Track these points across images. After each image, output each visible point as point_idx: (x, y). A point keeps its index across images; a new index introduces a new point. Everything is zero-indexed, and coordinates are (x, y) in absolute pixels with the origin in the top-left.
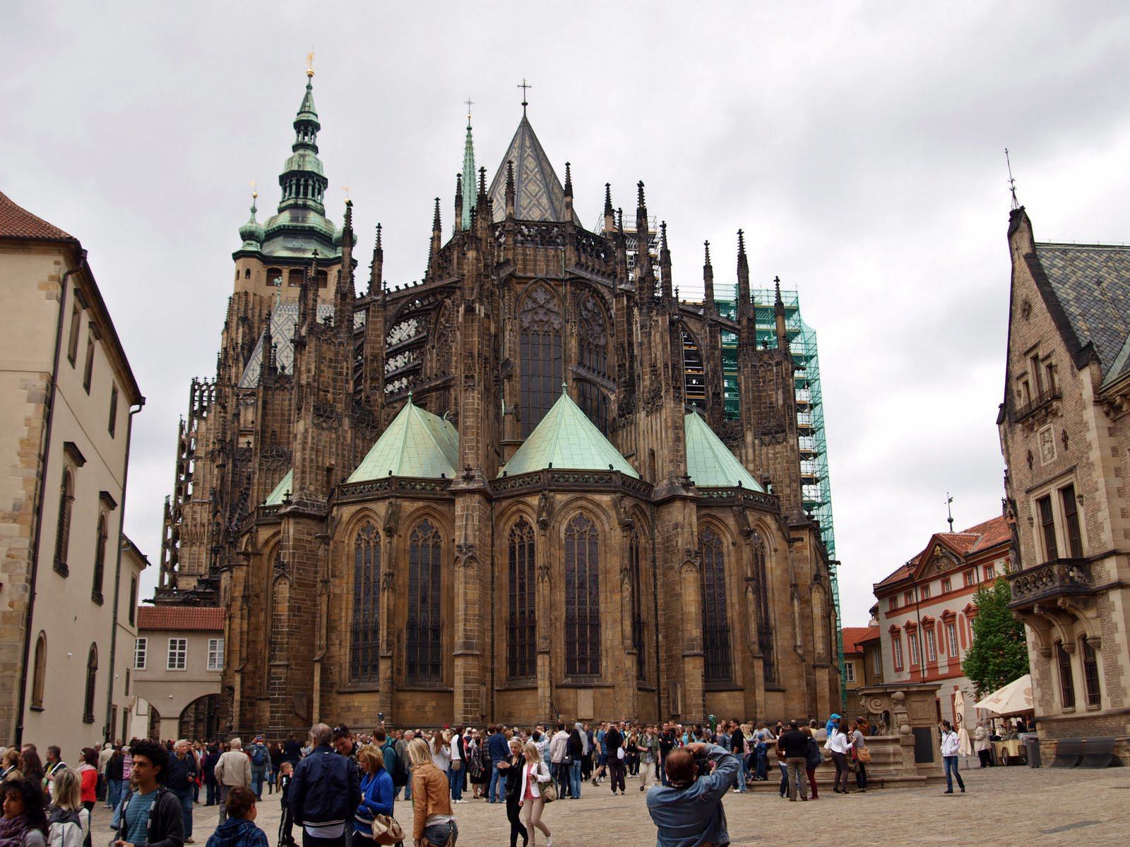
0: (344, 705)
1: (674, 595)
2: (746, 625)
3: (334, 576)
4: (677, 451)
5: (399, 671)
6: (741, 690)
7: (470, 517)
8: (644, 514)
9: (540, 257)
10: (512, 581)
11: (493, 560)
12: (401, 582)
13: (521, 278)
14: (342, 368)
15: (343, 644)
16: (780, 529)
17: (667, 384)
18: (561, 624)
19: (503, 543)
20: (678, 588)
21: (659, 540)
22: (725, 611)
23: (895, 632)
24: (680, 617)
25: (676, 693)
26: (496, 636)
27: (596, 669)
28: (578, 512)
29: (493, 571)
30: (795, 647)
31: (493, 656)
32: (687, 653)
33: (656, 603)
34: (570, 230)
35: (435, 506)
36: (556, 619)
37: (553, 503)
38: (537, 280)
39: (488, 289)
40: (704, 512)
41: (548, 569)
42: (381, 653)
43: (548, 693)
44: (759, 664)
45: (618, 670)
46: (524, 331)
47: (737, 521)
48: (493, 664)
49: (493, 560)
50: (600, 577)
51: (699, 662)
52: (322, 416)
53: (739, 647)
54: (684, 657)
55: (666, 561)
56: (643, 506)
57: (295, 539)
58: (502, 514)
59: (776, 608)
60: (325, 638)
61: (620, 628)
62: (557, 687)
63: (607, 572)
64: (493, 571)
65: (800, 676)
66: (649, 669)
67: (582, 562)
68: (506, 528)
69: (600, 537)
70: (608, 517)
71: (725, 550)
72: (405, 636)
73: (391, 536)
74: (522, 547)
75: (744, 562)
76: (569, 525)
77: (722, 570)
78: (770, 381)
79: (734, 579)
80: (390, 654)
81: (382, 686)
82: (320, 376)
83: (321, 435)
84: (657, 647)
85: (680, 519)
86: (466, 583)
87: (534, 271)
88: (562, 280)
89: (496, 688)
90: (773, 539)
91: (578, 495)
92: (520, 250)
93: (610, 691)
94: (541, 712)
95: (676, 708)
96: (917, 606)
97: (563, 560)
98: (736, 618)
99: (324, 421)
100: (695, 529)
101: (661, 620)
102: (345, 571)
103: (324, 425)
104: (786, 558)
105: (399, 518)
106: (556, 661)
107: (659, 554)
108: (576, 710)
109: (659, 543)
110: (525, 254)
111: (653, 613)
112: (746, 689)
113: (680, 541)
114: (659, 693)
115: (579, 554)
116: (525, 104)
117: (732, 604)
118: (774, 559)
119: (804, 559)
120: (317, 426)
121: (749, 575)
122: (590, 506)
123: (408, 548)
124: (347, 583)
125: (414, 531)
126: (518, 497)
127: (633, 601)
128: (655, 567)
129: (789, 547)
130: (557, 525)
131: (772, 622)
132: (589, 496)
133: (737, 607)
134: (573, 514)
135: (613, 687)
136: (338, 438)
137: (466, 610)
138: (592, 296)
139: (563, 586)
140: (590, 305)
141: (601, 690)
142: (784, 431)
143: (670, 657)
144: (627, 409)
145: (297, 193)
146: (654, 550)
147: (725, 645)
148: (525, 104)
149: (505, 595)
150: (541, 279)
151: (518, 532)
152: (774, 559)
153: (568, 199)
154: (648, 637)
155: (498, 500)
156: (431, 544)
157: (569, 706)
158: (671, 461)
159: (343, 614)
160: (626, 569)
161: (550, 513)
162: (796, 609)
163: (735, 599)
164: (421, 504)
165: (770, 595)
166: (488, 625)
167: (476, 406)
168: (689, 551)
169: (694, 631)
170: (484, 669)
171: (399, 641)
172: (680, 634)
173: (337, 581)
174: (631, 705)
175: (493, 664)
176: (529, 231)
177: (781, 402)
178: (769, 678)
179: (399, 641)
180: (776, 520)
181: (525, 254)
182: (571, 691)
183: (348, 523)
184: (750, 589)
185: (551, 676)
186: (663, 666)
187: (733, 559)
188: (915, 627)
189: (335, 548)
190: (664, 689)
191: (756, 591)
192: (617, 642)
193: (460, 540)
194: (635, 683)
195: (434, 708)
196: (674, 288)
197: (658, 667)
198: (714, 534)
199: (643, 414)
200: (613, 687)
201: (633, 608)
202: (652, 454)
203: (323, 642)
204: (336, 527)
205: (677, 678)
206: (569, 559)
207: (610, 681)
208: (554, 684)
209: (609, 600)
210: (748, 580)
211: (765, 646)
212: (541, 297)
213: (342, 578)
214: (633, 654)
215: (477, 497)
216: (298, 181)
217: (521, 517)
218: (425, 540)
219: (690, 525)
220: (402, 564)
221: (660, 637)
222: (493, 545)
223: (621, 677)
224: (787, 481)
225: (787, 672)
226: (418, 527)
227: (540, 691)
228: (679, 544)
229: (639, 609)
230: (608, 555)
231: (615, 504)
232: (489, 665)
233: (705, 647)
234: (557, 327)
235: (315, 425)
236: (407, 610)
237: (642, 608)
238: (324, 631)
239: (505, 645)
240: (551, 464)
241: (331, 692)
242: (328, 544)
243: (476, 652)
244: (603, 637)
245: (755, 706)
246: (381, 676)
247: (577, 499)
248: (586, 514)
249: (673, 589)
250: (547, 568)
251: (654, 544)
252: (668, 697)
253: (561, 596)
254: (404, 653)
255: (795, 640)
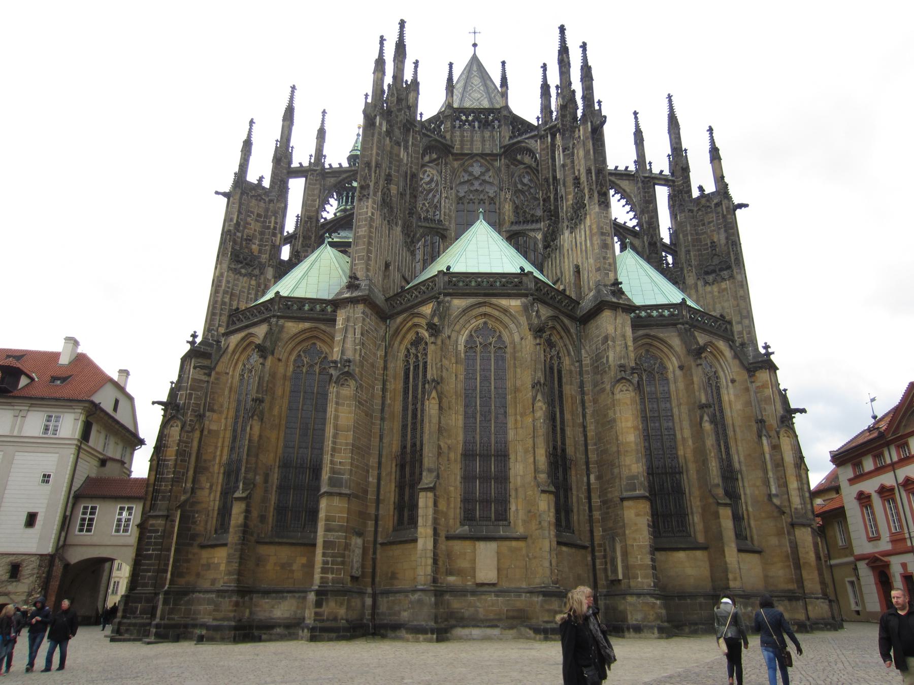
0: (204, 561)
1: (607, 423)
2: (703, 462)
3: (212, 410)
4: (604, 258)
5: (263, 518)
6: (704, 548)
7: (351, 331)
8: (566, 329)
9: (477, 137)
10: (405, 409)
11: (384, 384)
12: (276, 411)
13: (457, 154)
14: (270, 222)
15: (214, 488)
16: (736, 356)
17: (591, 190)
18: (456, 455)
19: (397, 366)
20: (611, 413)
21: (587, 361)
22: (675, 448)
23: (864, 499)
24: (614, 449)
25: (614, 551)
26: (384, 474)
27: (503, 516)
28: (482, 321)
29: (384, 397)
30: (770, 496)
31: (378, 501)
32: (625, 494)
33: (586, 436)
34: (505, 113)
35: (323, 327)
36: (449, 448)
37: (448, 308)
38: (472, 156)
39: (401, 121)
40: (641, 332)
41: (438, 383)
42: (236, 495)
43: (430, 545)
44: (726, 515)
45: (532, 515)
46: (460, 200)
47: (684, 342)
48: (377, 509)
49: (384, 384)
50: (509, 397)
51: (645, 507)
52: (241, 263)
53: (696, 492)
54: (622, 499)
55: (595, 385)
56: (566, 321)
57: (194, 380)
58: (397, 332)
59: (740, 448)
60: (190, 480)
61: (531, 460)
62: (448, 538)
63: (516, 390)
64: (384, 397)
65: (780, 533)
66: (578, 517)
67: (485, 379)
68: (401, 349)
69: (509, 350)
70: (518, 325)
71: (671, 376)
72: (276, 476)
73: (264, 357)
74: (416, 367)
75: (696, 386)
76: (471, 336)
77: (668, 399)
78: (709, 223)
79: (684, 409)
80: (244, 495)
81: (232, 537)
82: (245, 228)
83: (238, 280)
84: (589, 490)
85: (610, 330)
86: (337, 403)
87: (471, 149)
88: (496, 155)
89: (380, 540)
90: (729, 369)
91: (481, 299)
92: (458, 133)
93: (521, 544)
94: (420, 571)
95: (615, 571)
96: (893, 466)
97: (462, 377)
98: (690, 456)
99: (242, 268)
100: (630, 343)
101: (593, 457)
102: (226, 405)
103: (243, 271)
104: (747, 389)
105: (278, 339)
106: (448, 505)
107: (587, 378)
108: (474, 569)
109: (587, 365)
110: (462, 136)
111: (582, 448)
112: (712, 546)
113: (611, 355)
114: (593, 551)
115: (483, 370)
116: (475, 45)
117: (683, 439)
118: (731, 391)
119: (767, 400)
120: (236, 271)
121: (704, 401)
122: (496, 313)
123: (289, 374)
124: (226, 418)
125: (299, 356)
126: (411, 309)
127: (554, 427)
128: (583, 393)
129: (750, 377)
130: (454, 335)
131: (737, 465)
132: (494, 300)
133: (690, 442)
134: (475, 323)
135: (523, 538)
136: (259, 285)
137: (335, 436)
138: (527, 173)
139: (461, 409)
140: (526, 181)
141: (507, 543)
142: (729, 267)
143: (604, 502)
144: (551, 239)
145: (347, 202)
146: (581, 373)
147: (678, 491)
148: (475, 45)
149: (397, 425)
150: (477, 155)
151: (413, 351)
152: (731, 391)
153: (504, 89)
154: (576, 478)
155: (392, 317)
156: (317, 371)
157: (463, 564)
158: (598, 270)
159: (218, 453)
160: (539, 382)
161: (442, 318)
162: (766, 448)
163: (687, 433)
164: (307, 325)
165: (730, 433)
166: (373, 461)
167: (370, 214)
168: (622, 367)
169: (633, 466)
170: (363, 515)
171: (266, 481)
172: (616, 471)
173: (215, 416)
174: (547, 564)
175: (377, 509)
176: (467, 117)
177: (723, 241)
178: (740, 536)
179: (266, 481)
180: (731, 347)
181: (462, 136)
182: (467, 543)
183: (234, 352)
184: (706, 418)
185: (435, 520)
186: (597, 515)
187: (681, 385)
188: (892, 490)
189: (217, 379)
190: (600, 545)
191: (713, 421)
192: (529, 478)
193: (336, 355)
194: (553, 533)
195: (303, 565)
196: (596, 100)
197: (591, 516)
198: (655, 358)
199: (567, 233)
200: (523, 538)
201: (555, 440)
202: (578, 271)
203: (189, 485)
204: (221, 357)
205: (615, 531)
206: (470, 376)
207: (521, 530)
208: (443, 534)
209: (519, 425)
210: (702, 407)
211: (733, 496)
212: (477, 170)
213: (221, 413)
214: (550, 492)
215: (360, 307)
216: (348, 194)
217: (417, 333)
218: (311, 366)
219: (624, 336)
220: (279, 392)
221: (592, 477)
222: (385, 368)
223: (534, 525)
224: (738, 319)
225: (761, 527)
226: (304, 352)
227: (421, 542)
228: (611, 359)
229: (564, 443)
230: (518, 370)
231: (526, 309)
232: (372, 511)
233: (651, 489)
234: (491, 194)
235: (229, 269)
236: (281, 444)
237: (568, 441)
238: (191, 473)
239: (393, 485)
240: (448, 268)
241: (191, 545)
242: (209, 375)
243: (345, 491)
244: (512, 472)
245: (726, 570)
246: (233, 522)
247: (480, 305)
248: (491, 323)
249: (606, 416)
250: (437, 382)
251: (581, 366)
252: (605, 557)
253: (456, 420)
254: (273, 498)
255: (768, 485)
